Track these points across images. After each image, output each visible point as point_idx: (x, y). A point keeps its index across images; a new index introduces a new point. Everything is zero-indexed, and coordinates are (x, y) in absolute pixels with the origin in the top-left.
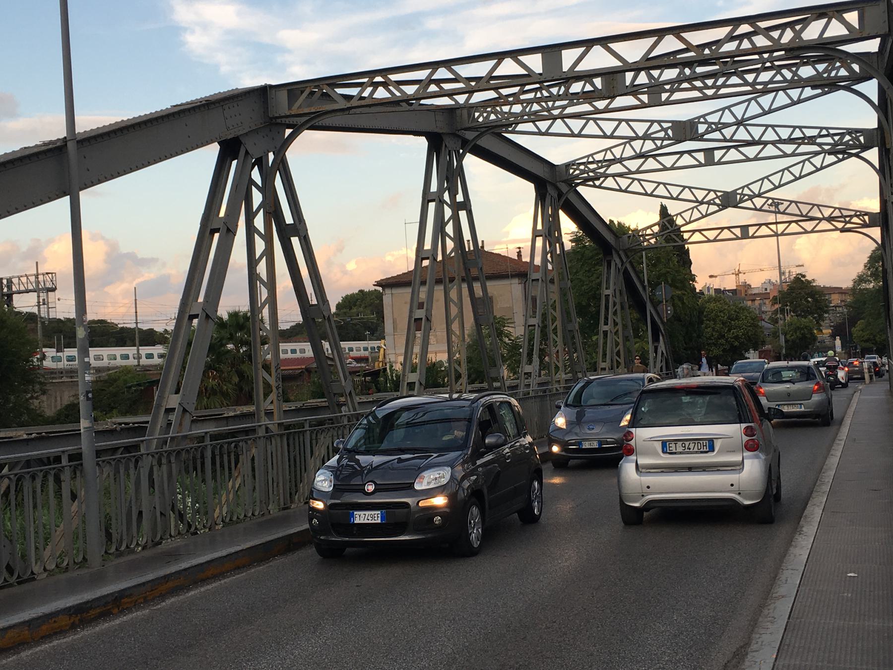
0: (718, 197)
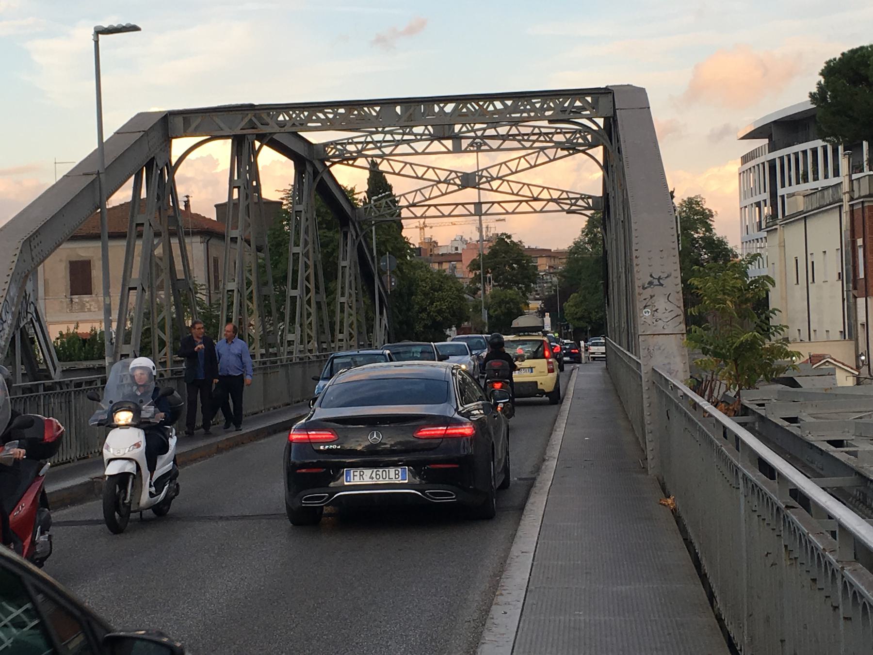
0: (458, 177)
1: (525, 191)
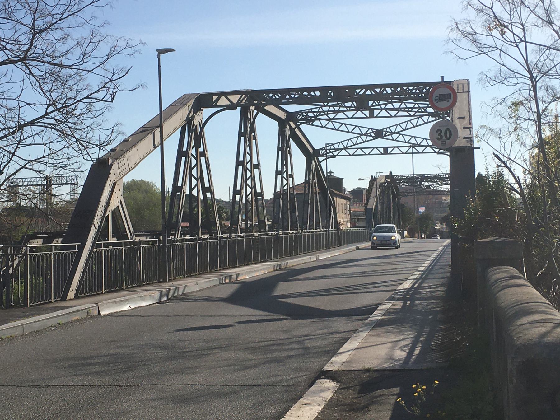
0: (373, 132)
1: (413, 141)
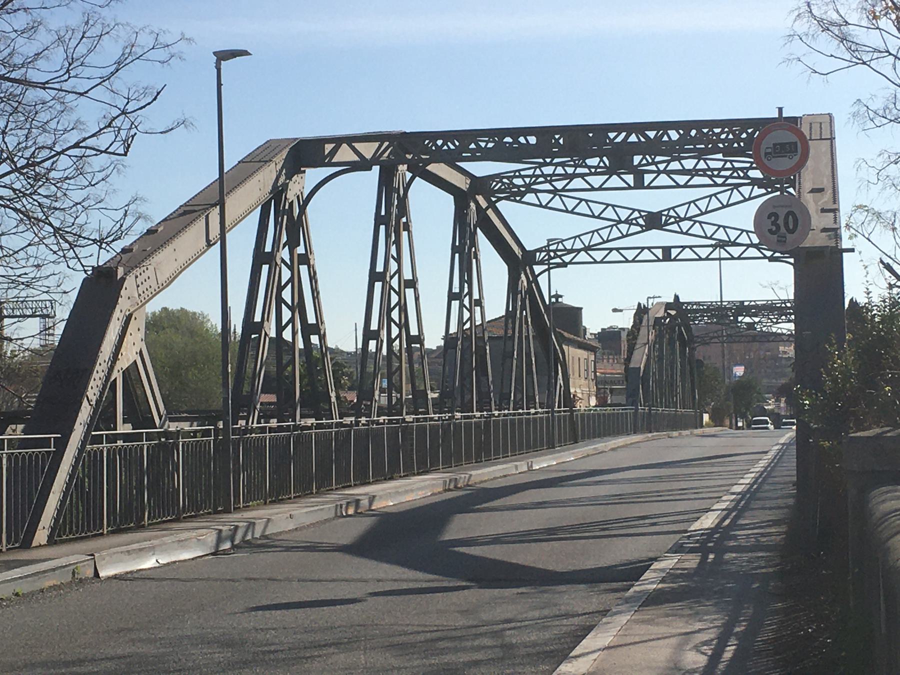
0: (641, 217)
1: (721, 235)
